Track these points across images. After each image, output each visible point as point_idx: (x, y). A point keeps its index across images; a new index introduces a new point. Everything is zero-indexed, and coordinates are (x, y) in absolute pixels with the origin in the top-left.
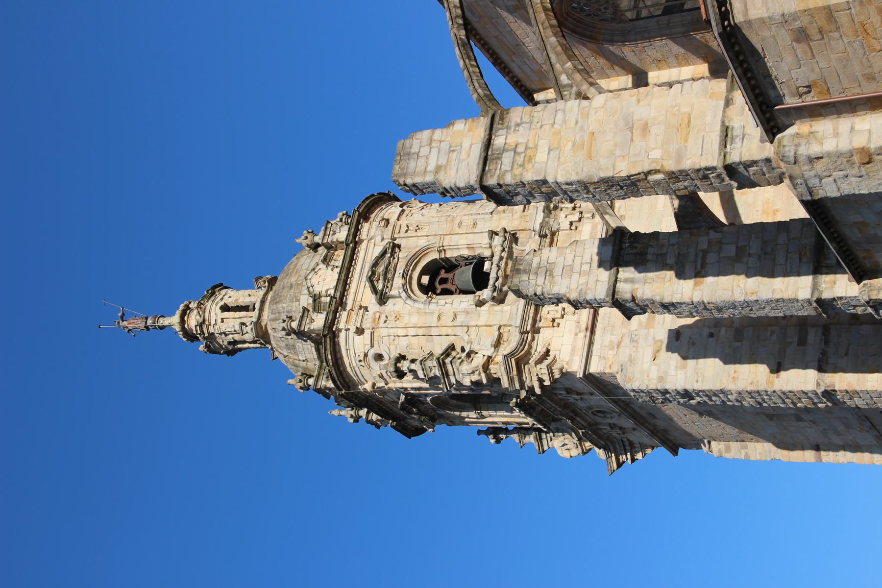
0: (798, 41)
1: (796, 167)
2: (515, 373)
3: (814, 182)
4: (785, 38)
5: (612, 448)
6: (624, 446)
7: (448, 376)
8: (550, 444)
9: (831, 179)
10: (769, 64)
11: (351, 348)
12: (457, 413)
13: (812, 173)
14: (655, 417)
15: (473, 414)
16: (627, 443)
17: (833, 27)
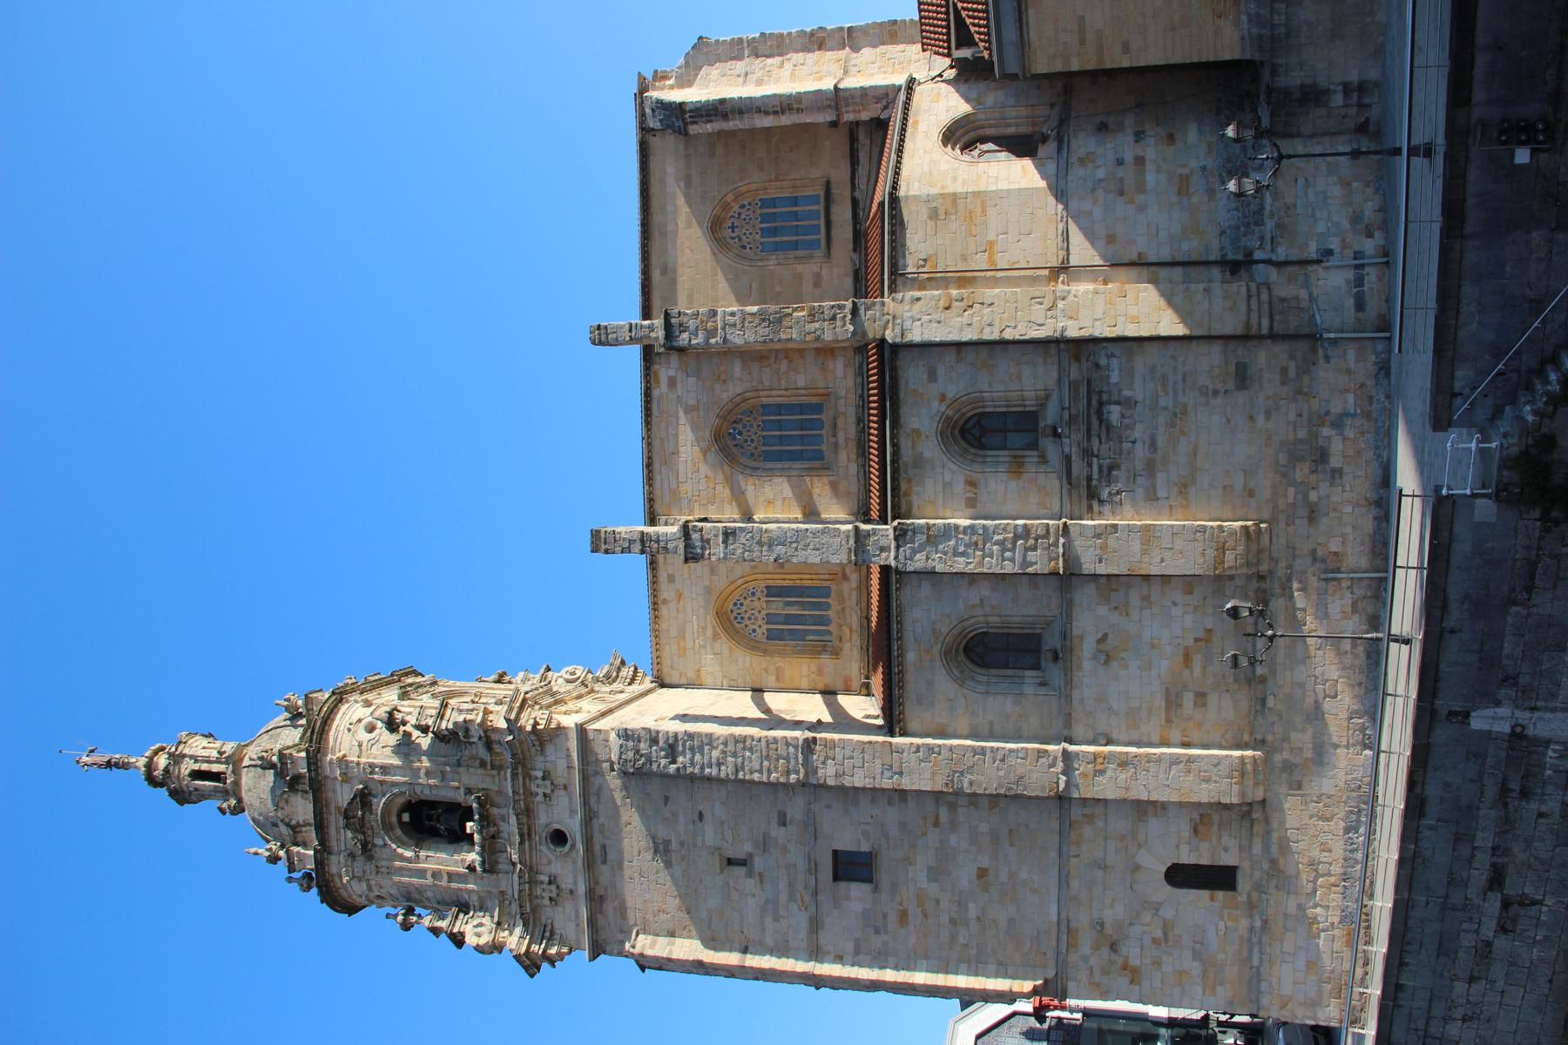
0: (931, 218)
1: (900, 306)
2: (518, 704)
3: (908, 324)
4: (924, 213)
5: (530, 929)
6: (544, 931)
7: (442, 719)
8: (463, 926)
9: (919, 323)
10: (908, 236)
11: (350, 713)
12: (394, 846)
13: (909, 314)
14: (605, 862)
15: (409, 854)
16: (549, 928)
17: (954, 210)
